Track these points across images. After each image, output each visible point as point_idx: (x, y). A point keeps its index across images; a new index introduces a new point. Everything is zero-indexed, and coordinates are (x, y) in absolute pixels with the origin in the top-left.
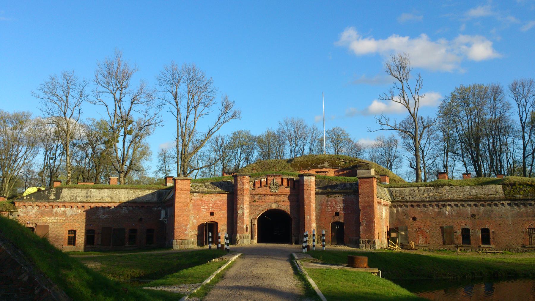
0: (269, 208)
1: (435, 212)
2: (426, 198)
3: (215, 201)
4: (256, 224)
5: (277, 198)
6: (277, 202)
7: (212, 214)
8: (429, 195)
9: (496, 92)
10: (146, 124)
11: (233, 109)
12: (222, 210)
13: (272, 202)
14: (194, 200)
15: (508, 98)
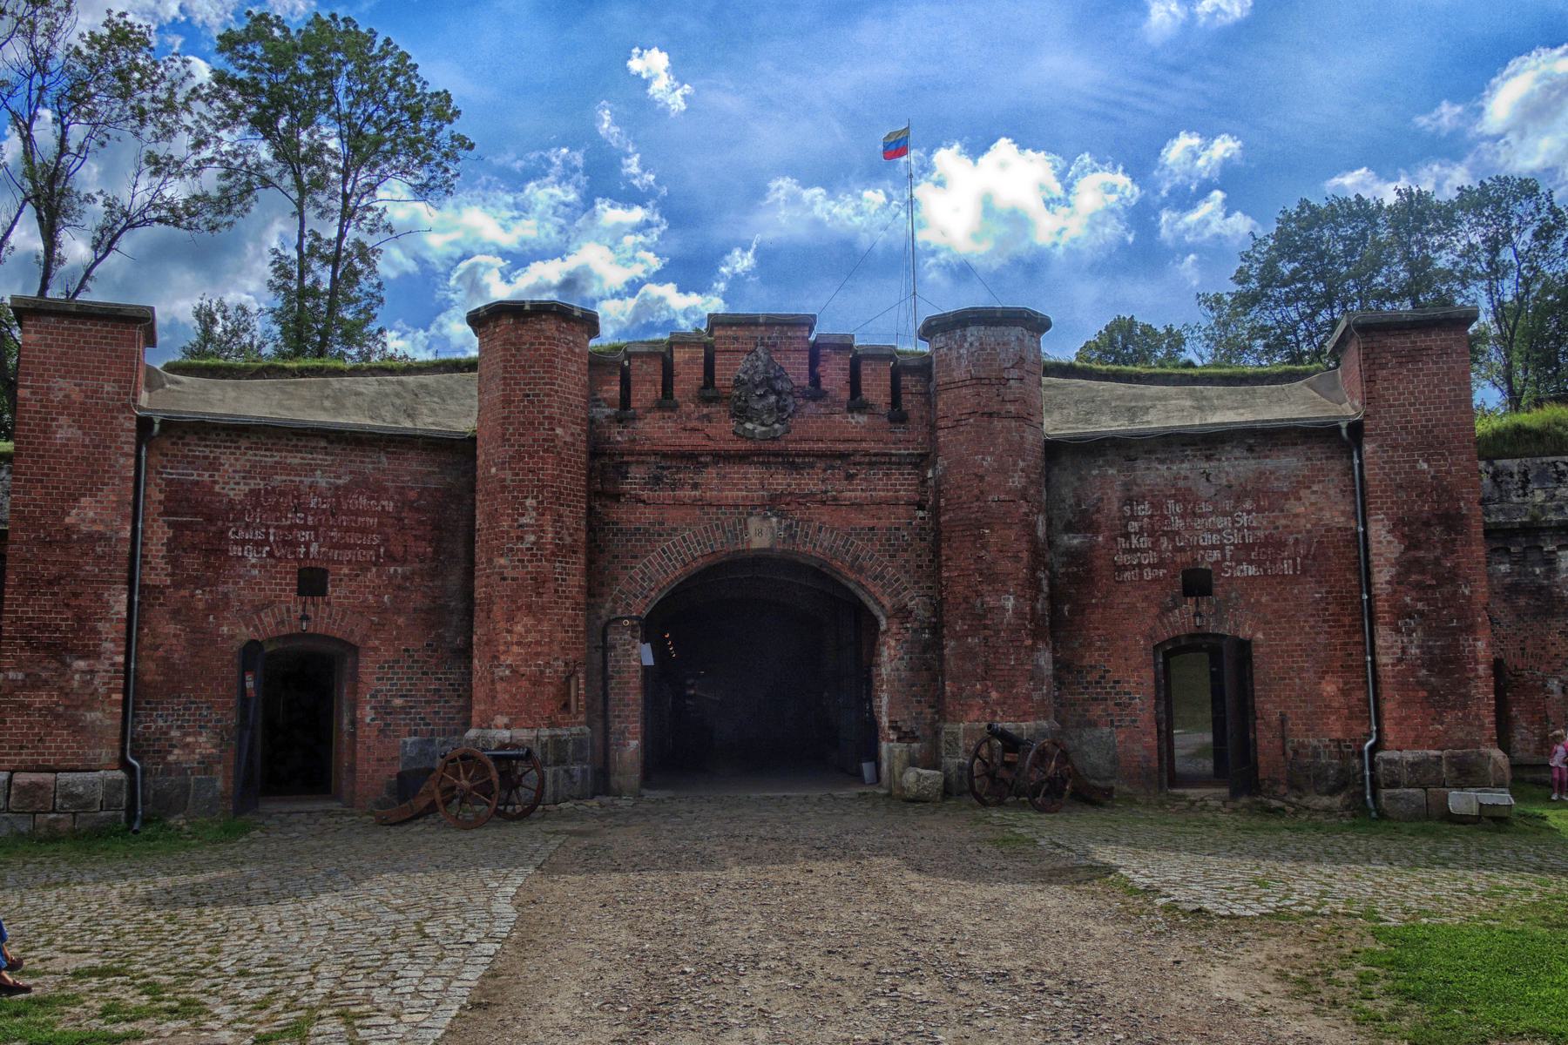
0: (721, 544)
5: (781, 481)
6: (773, 504)
7: (312, 582)
8: (1552, 497)
12: (391, 558)
13: (752, 508)
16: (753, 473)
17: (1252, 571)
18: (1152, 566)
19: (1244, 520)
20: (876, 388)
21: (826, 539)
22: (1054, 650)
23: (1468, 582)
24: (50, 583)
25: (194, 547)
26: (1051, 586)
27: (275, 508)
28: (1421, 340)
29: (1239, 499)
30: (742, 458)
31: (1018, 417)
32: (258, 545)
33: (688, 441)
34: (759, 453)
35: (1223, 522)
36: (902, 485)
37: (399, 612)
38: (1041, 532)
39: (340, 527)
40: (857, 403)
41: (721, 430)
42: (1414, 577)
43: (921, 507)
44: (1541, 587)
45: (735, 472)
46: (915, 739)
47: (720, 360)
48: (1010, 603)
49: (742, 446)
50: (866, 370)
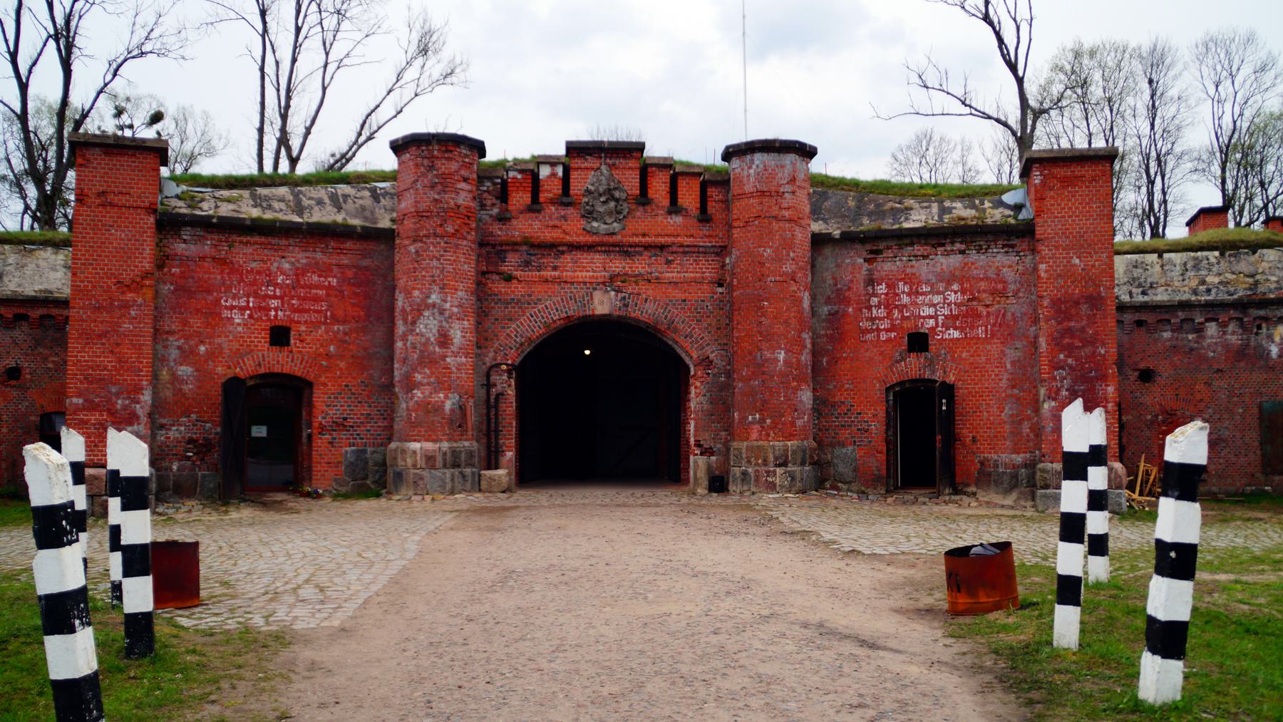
0: (573, 310)
1: (1226, 346)
2: (1195, 292)
3: (299, 273)
4: (511, 392)
5: (618, 265)
6: (612, 281)
8: (1203, 282)
9: (1155, 62)
10: (135, 53)
11: (446, 54)
12: (335, 320)
13: (594, 285)
14: (184, 260)
15: (1185, 81)
16: (598, 259)
17: (956, 334)
18: (887, 330)
19: (952, 298)
20: (689, 197)
21: (650, 308)
22: (814, 390)
23: (1104, 345)
24: (100, 337)
25: (198, 311)
26: (813, 344)
27: (254, 283)
28: (1078, 170)
29: (949, 283)
30: (590, 248)
31: (790, 220)
32: (242, 309)
33: (549, 235)
34: (601, 244)
35: (937, 299)
36: (706, 269)
37: (342, 357)
38: (806, 304)
39: (299, 298)
40: (674, 207)
41: (573, 227)
42: (1066, 341)
43: (721, 285)
44: (1192, 350)
45: (585, 258)
46: (712, 454)
47: (574, 175)
48: (782, 356)
49: (589, 239)
50: (682, 183)
